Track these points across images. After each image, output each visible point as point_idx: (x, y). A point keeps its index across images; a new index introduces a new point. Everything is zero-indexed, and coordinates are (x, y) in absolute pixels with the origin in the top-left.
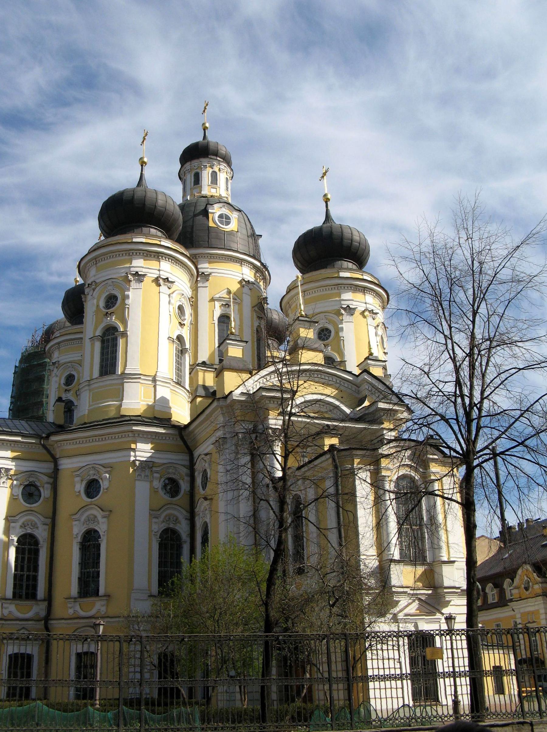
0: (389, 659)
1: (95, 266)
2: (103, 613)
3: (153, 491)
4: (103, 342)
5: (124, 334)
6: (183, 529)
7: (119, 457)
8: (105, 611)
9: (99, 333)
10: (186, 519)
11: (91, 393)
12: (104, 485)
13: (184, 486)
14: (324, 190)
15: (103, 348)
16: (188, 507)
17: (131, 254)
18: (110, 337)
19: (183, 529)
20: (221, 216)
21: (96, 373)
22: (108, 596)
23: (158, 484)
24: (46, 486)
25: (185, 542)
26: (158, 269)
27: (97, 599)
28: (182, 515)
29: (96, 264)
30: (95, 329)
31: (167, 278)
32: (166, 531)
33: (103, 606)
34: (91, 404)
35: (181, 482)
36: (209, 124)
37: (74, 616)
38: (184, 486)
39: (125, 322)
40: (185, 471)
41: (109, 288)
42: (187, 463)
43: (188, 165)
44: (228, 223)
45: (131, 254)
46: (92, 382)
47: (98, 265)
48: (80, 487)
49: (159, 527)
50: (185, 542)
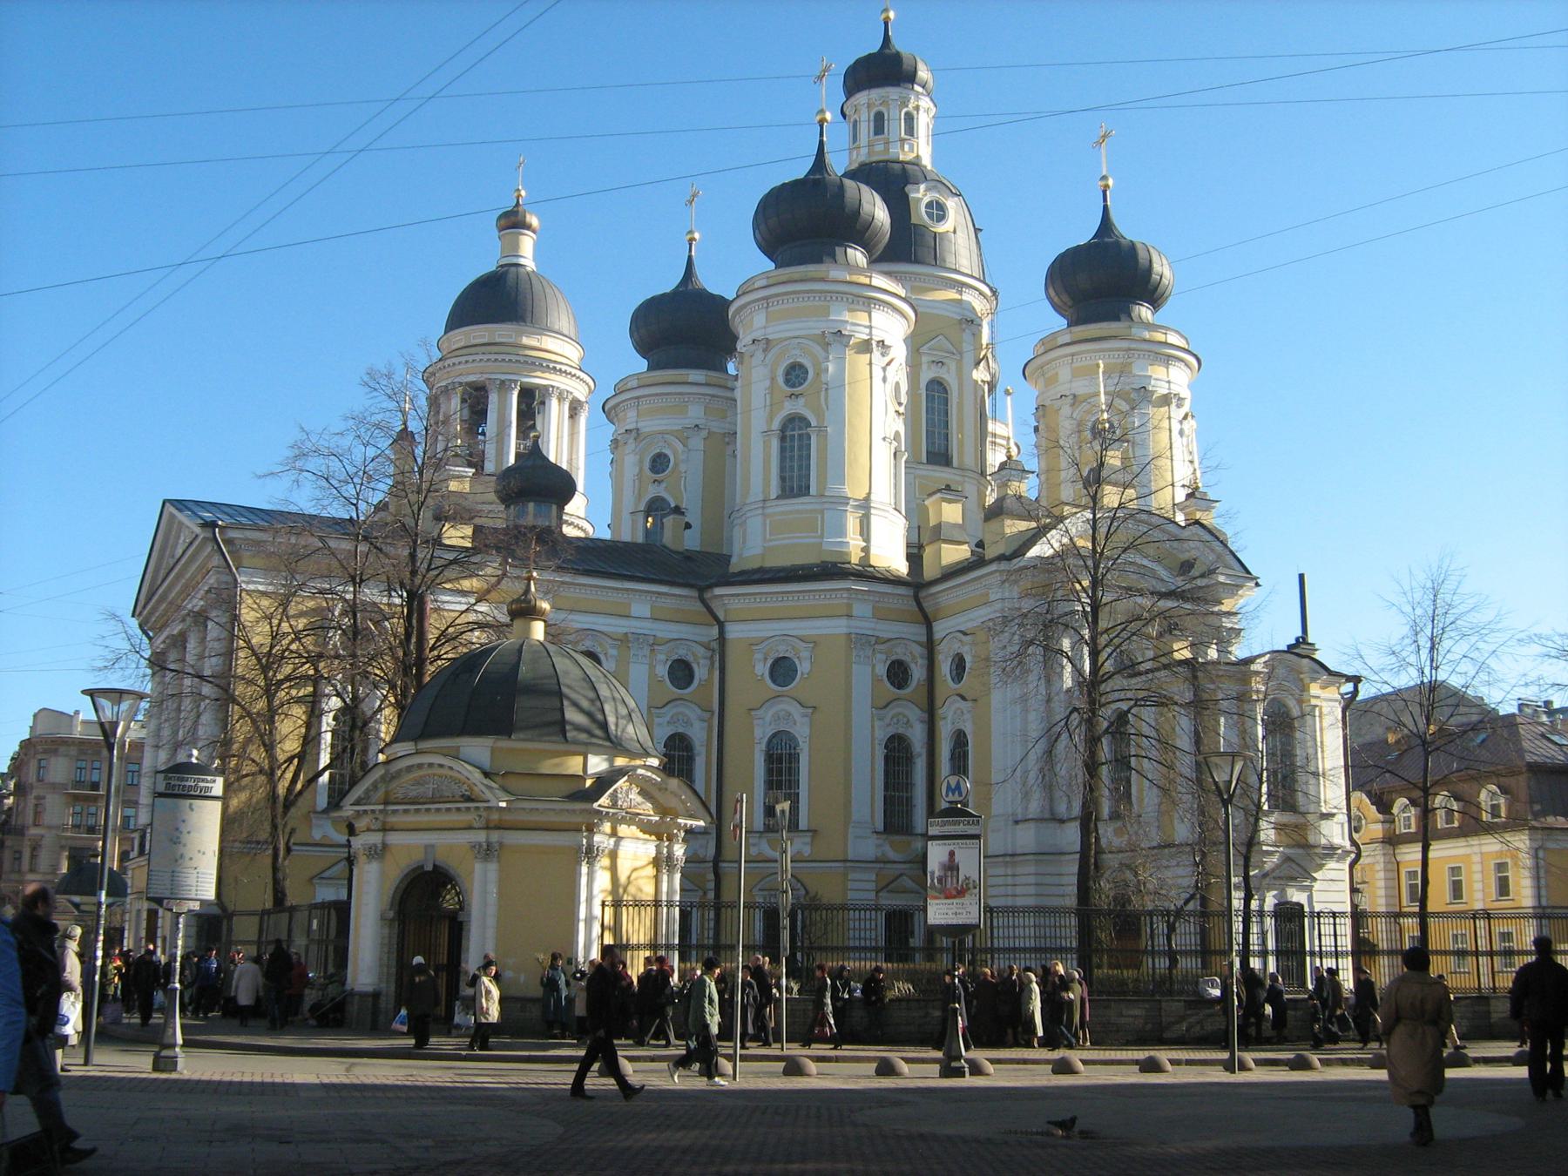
0: (1014, 937)
1: (764, 310)
2: (806, 855)
3: (876, 680)
4: (783, 439)
5: (822, 430)
6: (917, 735)
7: (818, 628)
8: (809, 852)
9: (776, 425)
10: (922, 722)
11: (768, 522)
12: (803, 667)
13: (918, 673)
14: (1102, 172)
15: (783, 450)
16: (925, 706)
17: (828, 298)
18: (796, 433)
19: (917, 735)
20: (930, 205)
21: (774, 491)
22: (813, 832)
23: (882, 670)
24: (702, 662)
25: (920, 755)
26: (868, 324)
27: (796, 834)
28: (915, 715)
29: (767, 308)
30: (771, 419)
31: (883, 341)
32: (892, 739)
33: (805, 844)
34: (768, 536)
35: (913, 666)
36: (896, 15)
37: (760, 859)
38: (918, 673)
39: (820, 415)
40: (918, 651)
41: (794, 352)
42: (924, 639)
43: (862, 98)
44: (941, 218)
45: (828, 298)
46: (768, 504)
47: (769, 309)
48: (763, 669)
49: (882, 735)
50: (920, 755)
